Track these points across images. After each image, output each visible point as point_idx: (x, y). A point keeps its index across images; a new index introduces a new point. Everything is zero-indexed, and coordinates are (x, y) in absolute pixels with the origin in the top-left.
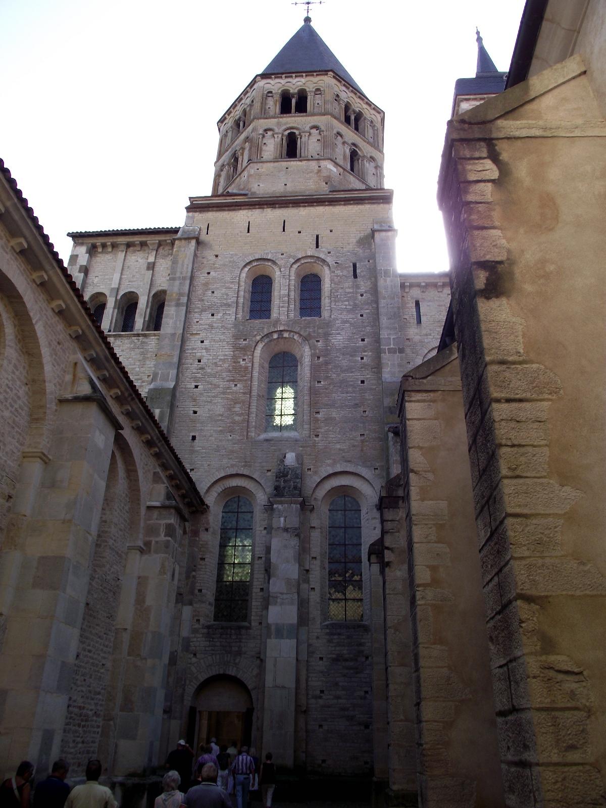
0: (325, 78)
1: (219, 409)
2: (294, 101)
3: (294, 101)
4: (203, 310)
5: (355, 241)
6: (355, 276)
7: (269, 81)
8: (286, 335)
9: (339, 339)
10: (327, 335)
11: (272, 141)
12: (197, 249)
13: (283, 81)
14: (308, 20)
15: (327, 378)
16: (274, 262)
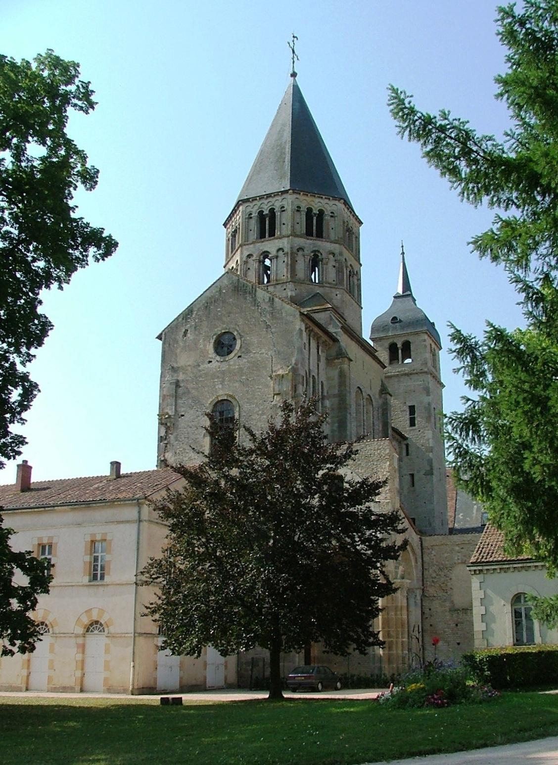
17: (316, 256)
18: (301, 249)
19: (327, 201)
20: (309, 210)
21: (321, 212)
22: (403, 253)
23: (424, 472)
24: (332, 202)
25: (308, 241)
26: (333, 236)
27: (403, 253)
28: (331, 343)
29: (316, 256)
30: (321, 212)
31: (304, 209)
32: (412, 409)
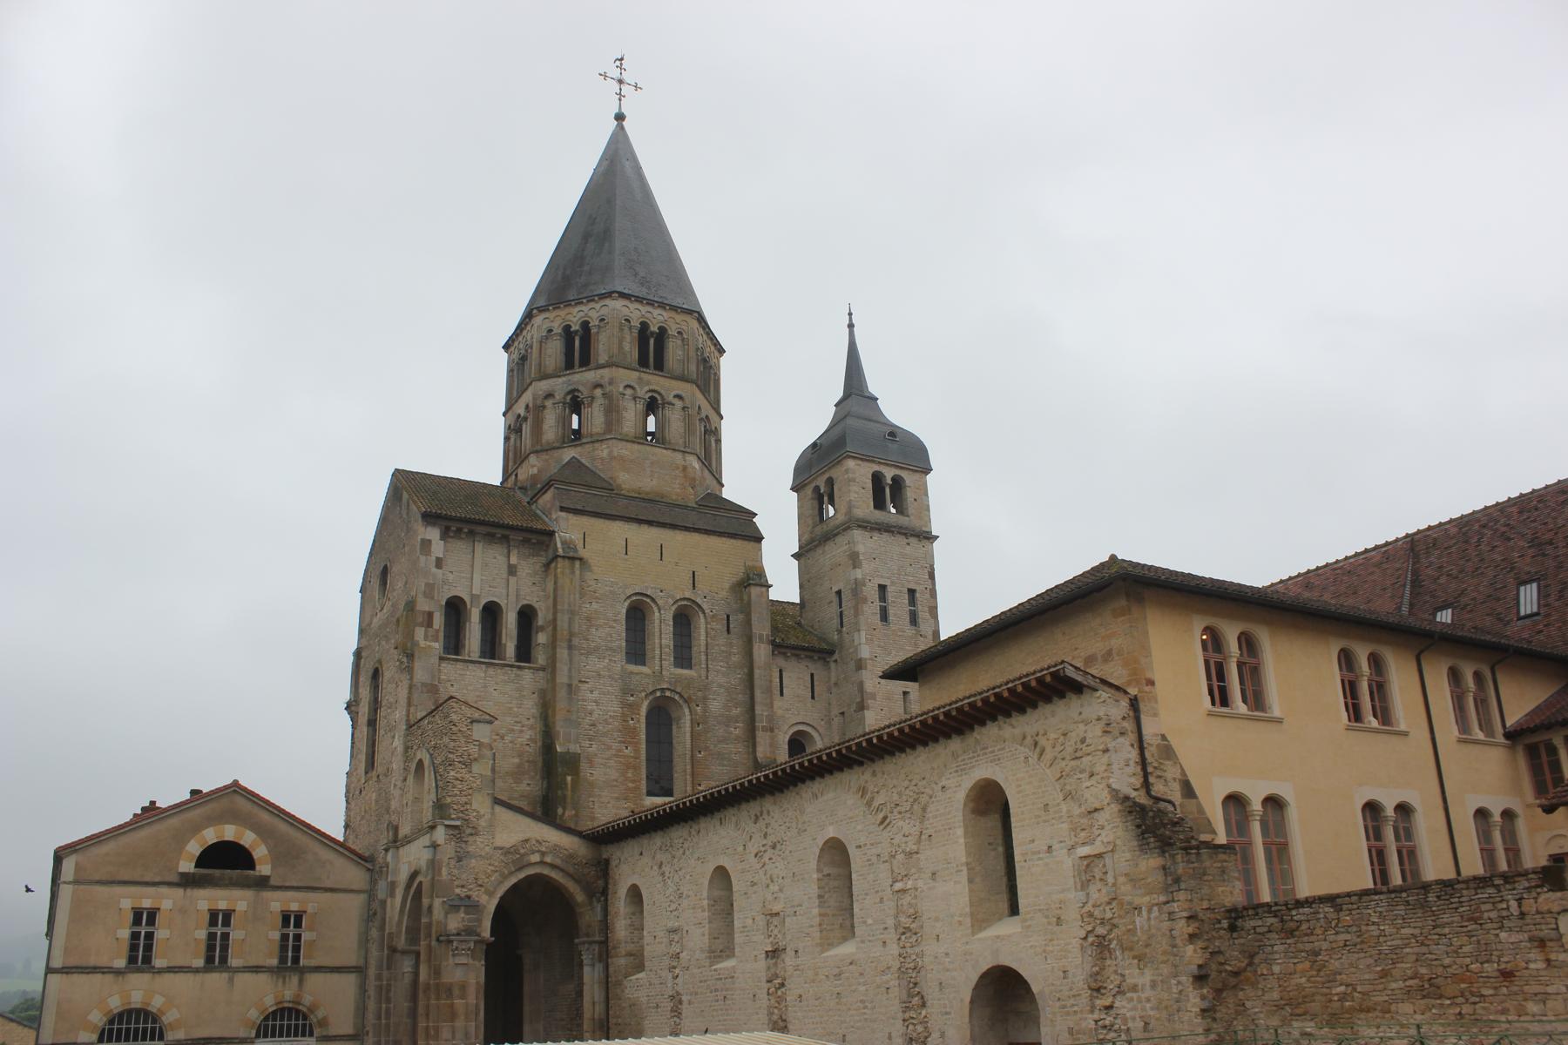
0: (687, 318)
1: (614, 774)
2: (652, 341)
3: (652, 341)
4: (589, 653)
5: (727, 586)
6: (728, 631)
7: (626, 302)
8: (668, 694)
9: (715, 706)
10: (705, 698)
11: (631, 405)
12: (581, 570)
13: (644, 309)
14: (620, 117)
15: (706, 749)
16: (653, 600)
17: (575, 398)
18: (549, 395)
19: (592, 305)
20: (567, 328)
21: (585, 325)
22: (851, 326)
23: (854, 707)
24: (598, 306)
25: (560, 380)
26: (603, 359)
27: (851, 326)
28: (545, 538)
29: (575, 398)
30: (585, 325)
31: (558, 330)
32: (839, 593)
